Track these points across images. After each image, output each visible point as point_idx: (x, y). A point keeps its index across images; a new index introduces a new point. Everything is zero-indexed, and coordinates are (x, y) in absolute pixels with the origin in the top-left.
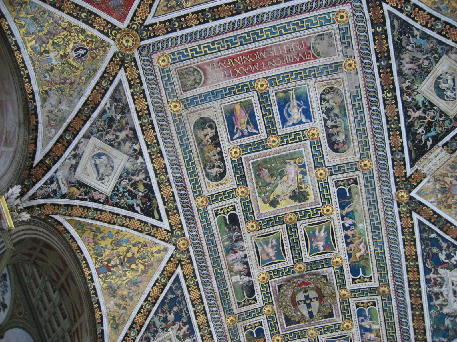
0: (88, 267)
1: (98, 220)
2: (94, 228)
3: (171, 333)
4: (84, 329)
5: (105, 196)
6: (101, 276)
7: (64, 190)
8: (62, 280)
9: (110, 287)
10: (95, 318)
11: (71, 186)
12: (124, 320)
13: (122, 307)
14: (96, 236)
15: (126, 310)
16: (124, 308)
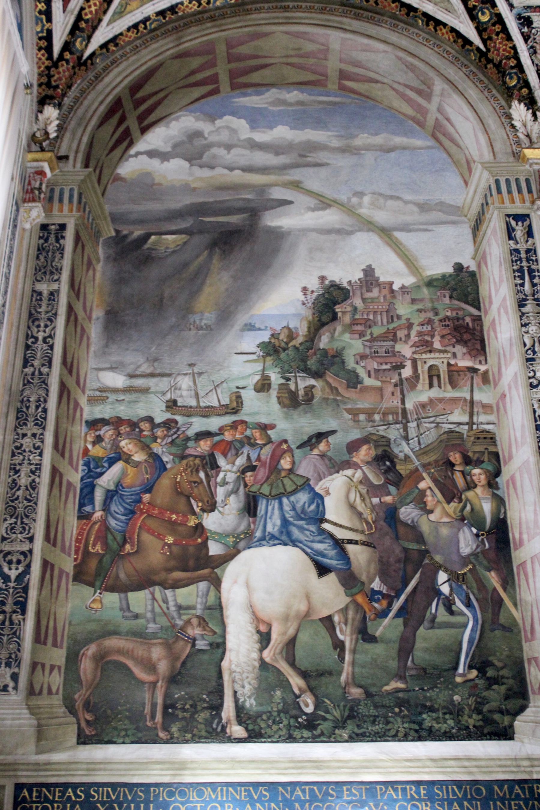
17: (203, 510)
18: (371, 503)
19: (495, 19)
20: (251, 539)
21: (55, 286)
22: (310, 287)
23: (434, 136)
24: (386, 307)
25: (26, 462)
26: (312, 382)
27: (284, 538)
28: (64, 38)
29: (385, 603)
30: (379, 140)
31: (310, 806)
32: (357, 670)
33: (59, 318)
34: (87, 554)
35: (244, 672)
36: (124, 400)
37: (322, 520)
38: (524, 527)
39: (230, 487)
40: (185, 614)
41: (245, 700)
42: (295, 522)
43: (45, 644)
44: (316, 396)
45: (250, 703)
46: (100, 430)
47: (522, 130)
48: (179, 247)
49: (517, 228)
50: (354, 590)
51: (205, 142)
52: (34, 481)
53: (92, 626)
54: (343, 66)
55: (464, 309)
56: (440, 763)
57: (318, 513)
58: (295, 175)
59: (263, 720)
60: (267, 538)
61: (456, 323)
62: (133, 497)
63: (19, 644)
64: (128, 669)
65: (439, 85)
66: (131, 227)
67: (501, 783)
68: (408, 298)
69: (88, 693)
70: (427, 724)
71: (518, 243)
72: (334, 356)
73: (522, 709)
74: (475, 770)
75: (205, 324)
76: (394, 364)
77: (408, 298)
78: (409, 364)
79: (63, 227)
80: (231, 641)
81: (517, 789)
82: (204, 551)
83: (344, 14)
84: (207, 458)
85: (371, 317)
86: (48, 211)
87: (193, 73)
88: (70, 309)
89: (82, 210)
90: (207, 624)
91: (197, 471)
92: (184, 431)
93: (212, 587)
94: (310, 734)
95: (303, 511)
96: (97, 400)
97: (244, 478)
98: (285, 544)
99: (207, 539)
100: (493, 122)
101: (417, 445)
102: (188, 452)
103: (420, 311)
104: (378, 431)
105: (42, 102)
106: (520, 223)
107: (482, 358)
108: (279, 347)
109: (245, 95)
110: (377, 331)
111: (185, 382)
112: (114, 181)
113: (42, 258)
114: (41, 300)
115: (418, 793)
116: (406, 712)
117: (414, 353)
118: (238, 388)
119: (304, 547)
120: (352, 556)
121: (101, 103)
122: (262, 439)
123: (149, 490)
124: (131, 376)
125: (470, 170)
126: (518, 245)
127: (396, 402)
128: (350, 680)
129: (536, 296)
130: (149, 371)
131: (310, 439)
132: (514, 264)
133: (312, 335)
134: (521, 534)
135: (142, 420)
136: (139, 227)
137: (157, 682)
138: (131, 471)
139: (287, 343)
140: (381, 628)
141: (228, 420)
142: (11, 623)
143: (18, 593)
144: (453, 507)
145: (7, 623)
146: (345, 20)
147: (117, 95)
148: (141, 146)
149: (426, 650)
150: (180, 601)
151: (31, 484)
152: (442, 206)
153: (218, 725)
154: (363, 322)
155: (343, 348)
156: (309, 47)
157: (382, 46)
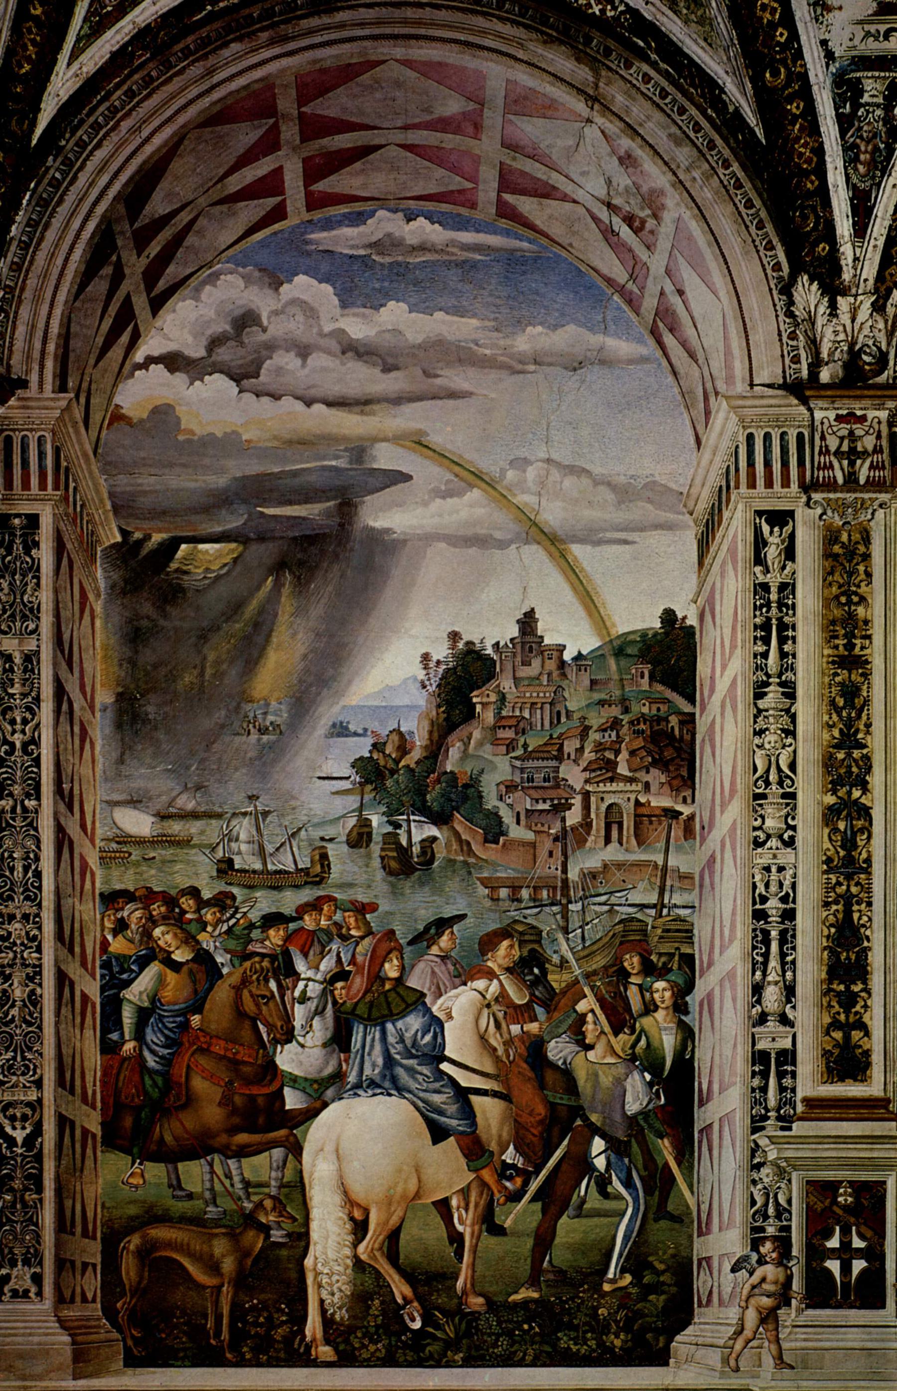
18: (510, 1033)
20: (342, 1087)
23: (654, 332)
26: (432, 831)
27: (387, 1084)
29: (519, 1181)
33: (43, 705)
35: (333, 1273)
36: (154, 858)
39: (312, 1005)
40: (256, 1194)
41: (335, 1312)
42: (405, 1062)
44: (437, 855)
45: (341, 1315)
46: (122, 909)
48: (226, 568)
49: (771, 540)
51: (263, 337)
52: (33, 992)
53: (132, 1210)
55: (669, 702)
57: (435, 1047)
59: (356, 1337)
60: (364, 1085)
61: (656, 728)
62: (178, 1019)
66: (146, 525)
69: (134, 1301)
71: (768, 572)
72: (466, 786)
75: (272, 723)
76: (556, 802)
78: (577, 801)
79: (33, 521)
82: (277, 1104)
84: (280, 957)
85: (526, 714)
89: (62, 487)
90: (285, 1207)
91: (267, 981)
92: (245, 913)
93: (290, 1156)
95: (415, 1043)
96: (115, 858)
97: (332, 992)
98: (390, 1095)
101: (579, 941)
103: (602, 703)
104: (525, 917)
106: (776, 529)
107: (688, 793)
108: (385, 767)
111: (244, 829)
114: (12, 670)
116: (537, 1330)
117: (587, 781)
118: (322, 839)
119: (415, 1099)
122: (358, 928)
123: (197, 1007)
124: (163, 817)
126: (769, 576)
128: (468, 1286)
129: (784, 678)
131: (427, 929)
132: (758, 613)
133: (434, 748)
134: (710, 1083)
135: (183, 892)
136: (160, 524)
137: (223, 1285)
138: (171, 977)
139: (397, 762)
141: (306, 895)
143: (28, 1163)
144: (624, 1039)
147: (103, 216)
149: (569, 1246)
150: (246, 1175)
151: (29, 996)
153: (300, 1345)
154: (513, 722)
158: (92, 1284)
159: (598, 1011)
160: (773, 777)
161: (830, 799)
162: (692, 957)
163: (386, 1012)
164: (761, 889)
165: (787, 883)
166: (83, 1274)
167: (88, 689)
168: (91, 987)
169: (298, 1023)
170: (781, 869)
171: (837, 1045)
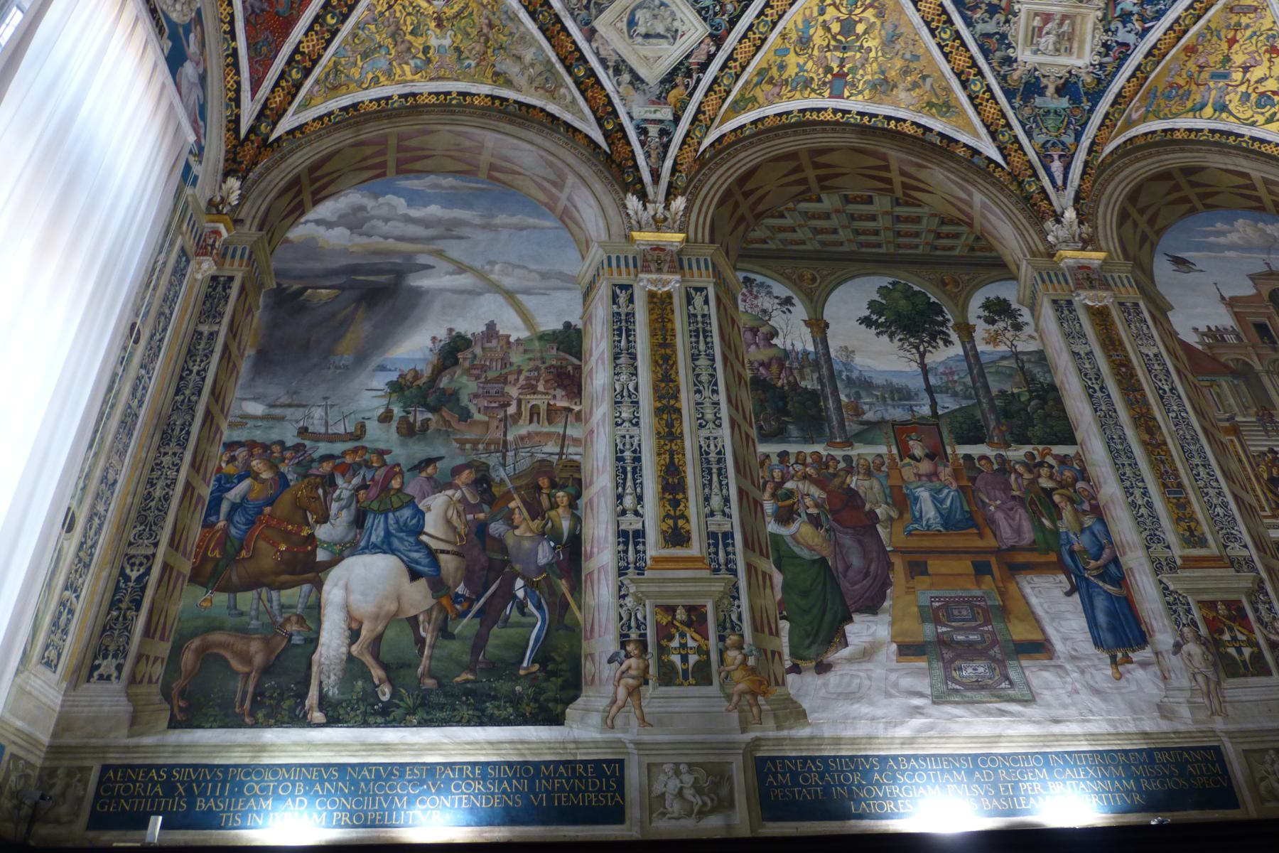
0: (819, 110)
1: (743, 68)
2: (755, 80)
3: (1024, 8)
4: (912, 170)
5: (708, 40)
6: (846, 94)
7: (666, 113)
8: (811, 174)
9: (874, 86)
10: (911, 136)
11: (665, 98)
12: (944, 89)
13: (920, 82)
14: (772, 78)
15: (928, 76)
16: (924, 78)
17: (317, 522)
19: (618, 127)
21: (215, 328)
22: (439, 337)
24: (501, 355)
25: (163, 477)
26: (429, 415)
27: (385, 547)
28: (251, 122)
29: (466, 605)
30: (515, 220)
31: (374, 785)
32: (433, 663)
33: (214, 354)
34: (205, 559)
37: (421, 532)
38: (595, 542)
39: (343, 503)
42: (398, 534)
43: (153, 637)
45: (333, 692)
47: (634, 217)
50: (440, 594)
51: (366, 215)
52: (167, 493)
53: (200, 623)
54: (493, 160)
56: (496, 746)
58: (439, 245)
63: (128, 638)
64: (226, 661)
65: (571, 179)
67: (547, 763)
68: (521, 349)
70: (490, 711)
72: (451, 395)
73: (575, 698)
74: (526, 752)
77: (521, 349)
78: (514, 403)
79: (231, 279)
80: (325, 637)
81: (562, 769)
83: (499, 120)
85: (488, 363)
86: (219, 264)
87: (365, 159)
88: (226, 347)
91: (317, 489)
93: (314, 589)
94: (383, 720)
95: (405, 523)
98: (385, 553)
99: (317, 547)
100: (612, 211)
102: (310, 472)
103: (530, 359)
105: (227, 174)
107: (578, 400)
109: (407, 179)
110: (491, 375)
112: (283, 242)
113: (208, 304)
114: (201, 339)
115: (473, 773)
120: (442, 564)
121: (282, 179)
122: (377, 462)
124: (271, 406)
125: (588, 247)
127: (499, 435)
130: (287, 402)
131: (420, 463)
135: (275, 443)
138: (257, 486)
139: (412, 383)
140: (460, 627)
141: (350, 445)
142: (125, 618)
145: (121, 619)
146: (501, 124)
148: (312, 215)
150: (283, 600)
152: (561, 276)
155: (460, 388)
156: (467, 143)
157: (528, 146)
158: (158, 670)
159: (521, 505)
160: (625, 393)
161: (659, 405)
162: (580, 480)
163: (389, 507)
164: (620, 446)
165: (635, 444)
166: (154, 663)
167: (242, 347)
168: (206, 491)
169: (333, 512)
170: (631, 437)
171: (670, 527)
